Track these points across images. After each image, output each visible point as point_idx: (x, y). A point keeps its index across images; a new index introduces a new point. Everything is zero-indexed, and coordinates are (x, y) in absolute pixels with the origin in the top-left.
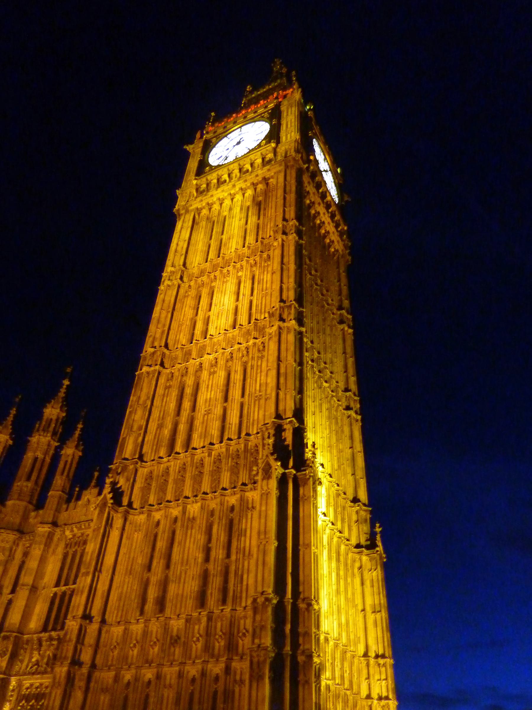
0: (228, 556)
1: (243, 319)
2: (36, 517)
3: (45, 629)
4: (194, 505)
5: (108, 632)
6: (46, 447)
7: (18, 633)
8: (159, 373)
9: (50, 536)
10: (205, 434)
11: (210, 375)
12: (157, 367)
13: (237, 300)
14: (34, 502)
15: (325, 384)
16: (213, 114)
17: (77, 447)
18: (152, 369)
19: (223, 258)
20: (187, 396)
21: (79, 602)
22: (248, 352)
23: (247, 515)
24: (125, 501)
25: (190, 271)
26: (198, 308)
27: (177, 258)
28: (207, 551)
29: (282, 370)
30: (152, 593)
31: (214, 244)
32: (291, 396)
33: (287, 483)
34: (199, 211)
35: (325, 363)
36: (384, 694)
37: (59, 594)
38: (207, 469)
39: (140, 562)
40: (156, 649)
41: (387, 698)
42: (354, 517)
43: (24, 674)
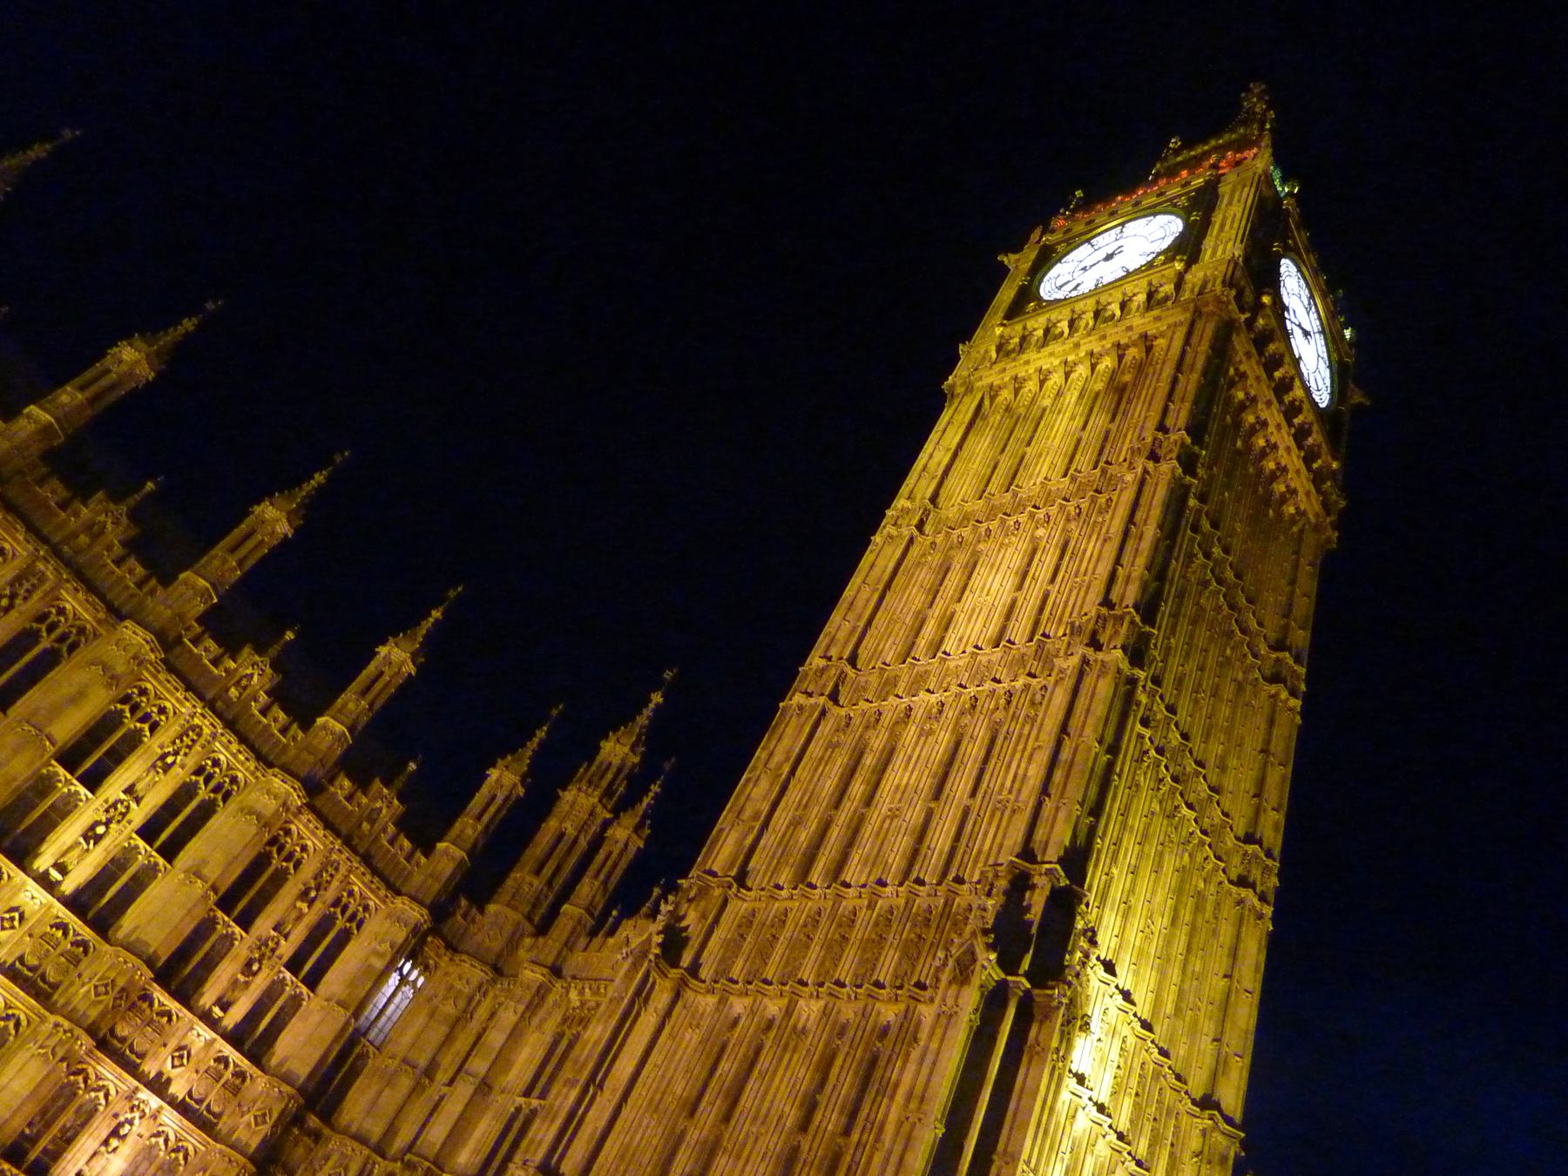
0: (847, 1132)
1: (1019, 630)
2: (530, 950)
4: (813, 1002)
7: (434, 1163)
8: (823, 713)
9: (541, 993)
10: (875, 859)
12: (822, 700)
13: (1020, 587)
14: (537, 919)
15: (1185, 810)
16: (1079, 193)
17: (637, 829)
18: (812, 701)
19: (1015, 495)
20: (865, 769)
21: (543, 1134)
22: (1009, 702)
23: (908, 1055)
24: (686, 959)
25: (943, 513)
27: (923, 482)
28: (810, 1108)
29: (1065, 755)
31: (1006, 464)
32: (1069, 815)
33: (1004, 1006)
34: (993, 391)
35: (1200, 763)
37: (525, 1111)
38: (856, 935)
39: (679, 1092)
42: (1195, 1143)
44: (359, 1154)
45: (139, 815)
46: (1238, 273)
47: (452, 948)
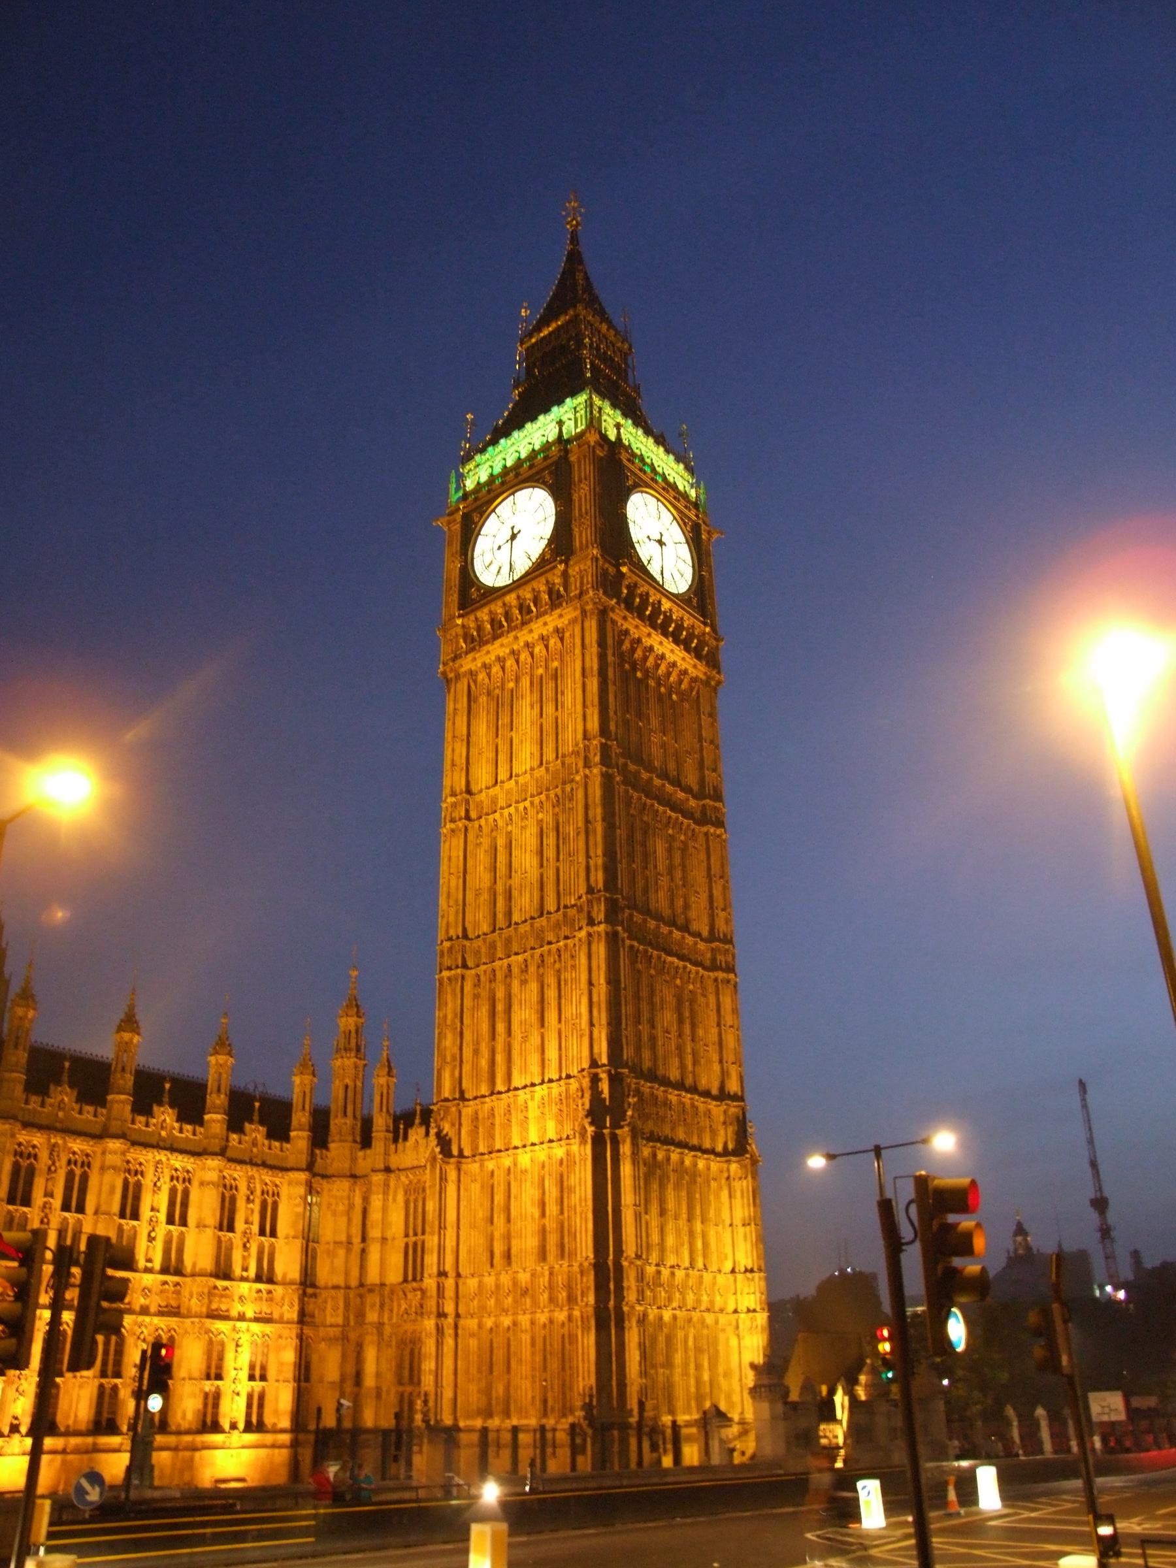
0: (562, 1212)
3: (405, 1280)
5: (464, 1283)
6: (353, 1071)
8: (463, 977)
12: (459, 971)
13: (542, 866)
14: (358, 1139)
22: (560, 956)
24: (455, 1152)
27: (456, 775)
28: (543, 1205)
29: (595, 999)
30: (499, 1249)
34: (472, 674)
36: (752, 1308)
40: (510, 1299)
45: (162, 1216)
46: (601, 562)
47: (324, 1176)
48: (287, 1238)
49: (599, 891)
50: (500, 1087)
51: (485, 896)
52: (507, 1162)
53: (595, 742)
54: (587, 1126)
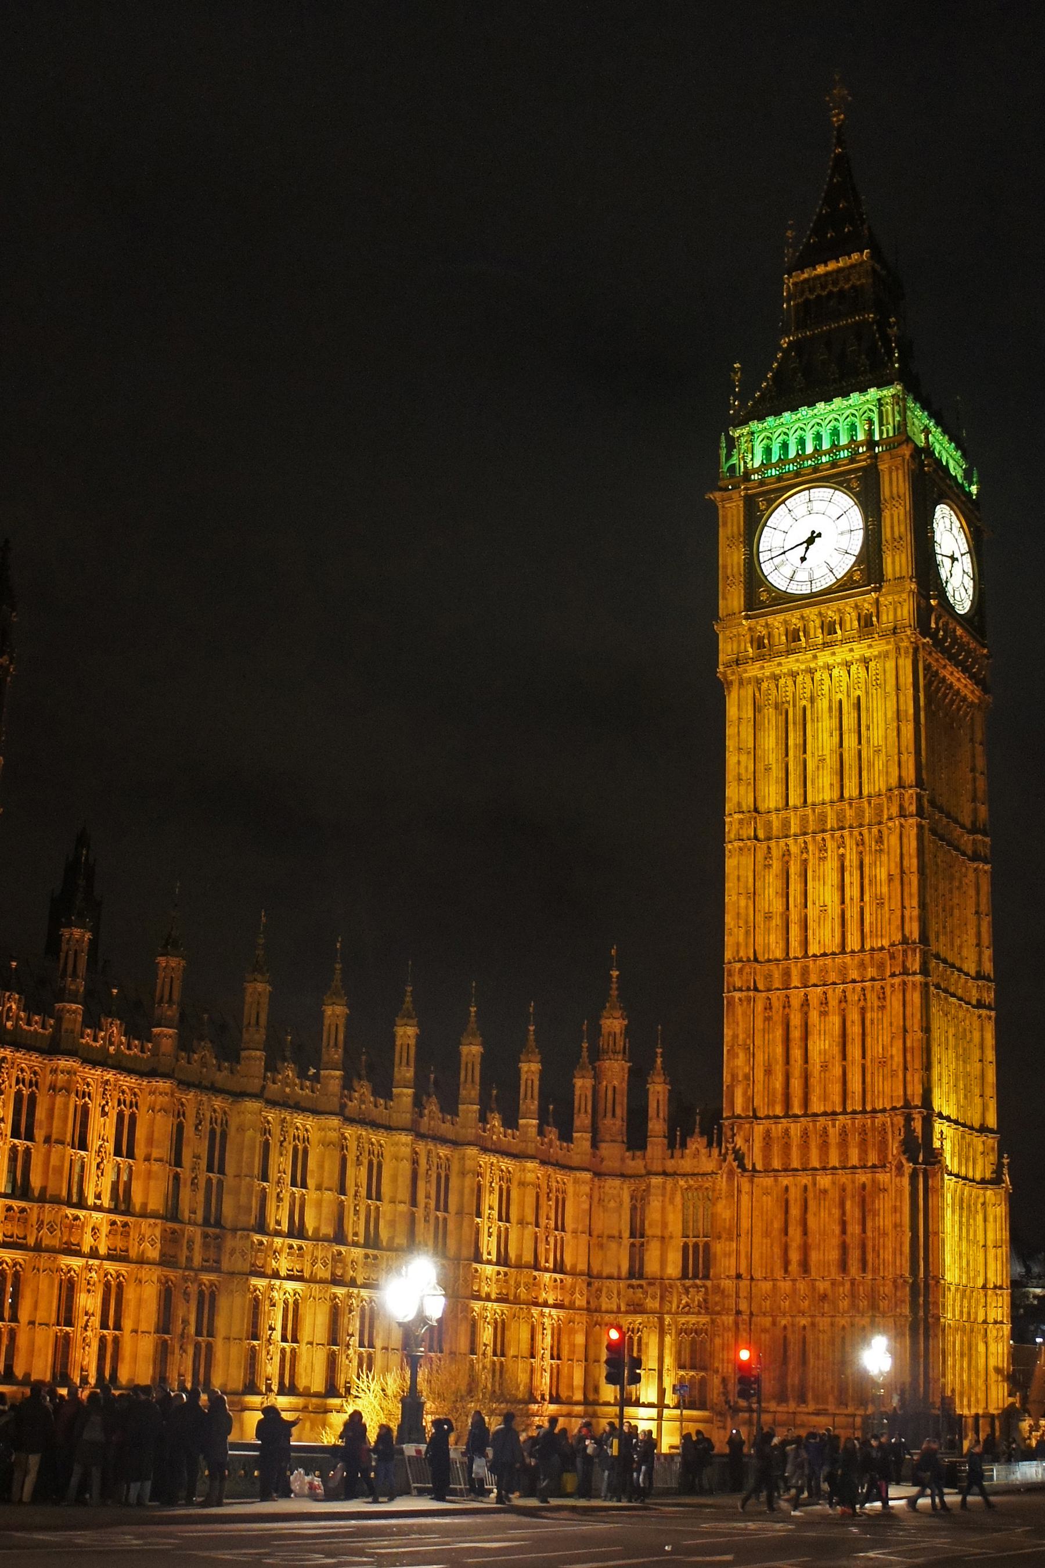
0: (864, 1231)
3: (685, 1276)
5: (756, 1285)
11: (820, 1016)
13: (843, 902)
26: (788, 893)
28: (843, 1224)
29: (909, 1044)
30: (795, 1256)
34: (758, 681)
36: (999, 1319)
41: (1002, 1322)
42: (980, 1148)
43: (677, 1313)
44: (613, 1284)
45: (495, 1214)
48: (575, 1232)
49: (914, 943)
50: (797, 1110)
51: (777, 921)
52: (805, 1179)
53: (910, 791)
54: (904, 1161)
